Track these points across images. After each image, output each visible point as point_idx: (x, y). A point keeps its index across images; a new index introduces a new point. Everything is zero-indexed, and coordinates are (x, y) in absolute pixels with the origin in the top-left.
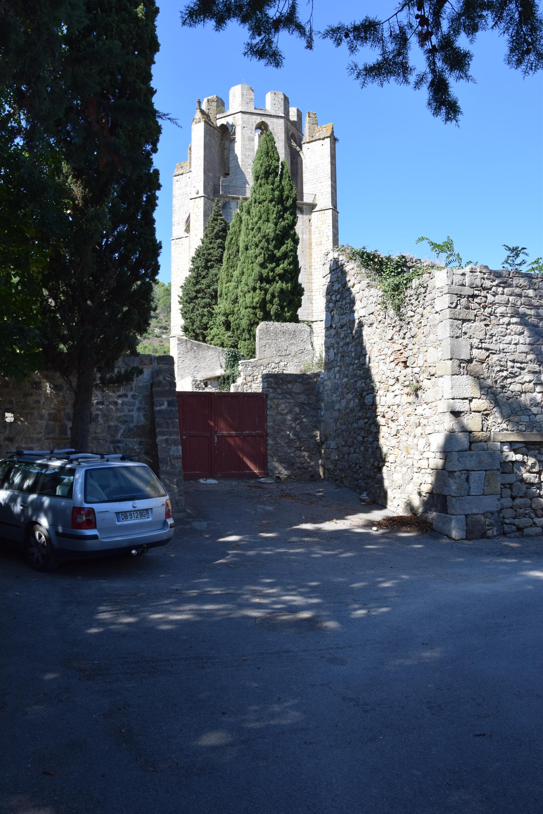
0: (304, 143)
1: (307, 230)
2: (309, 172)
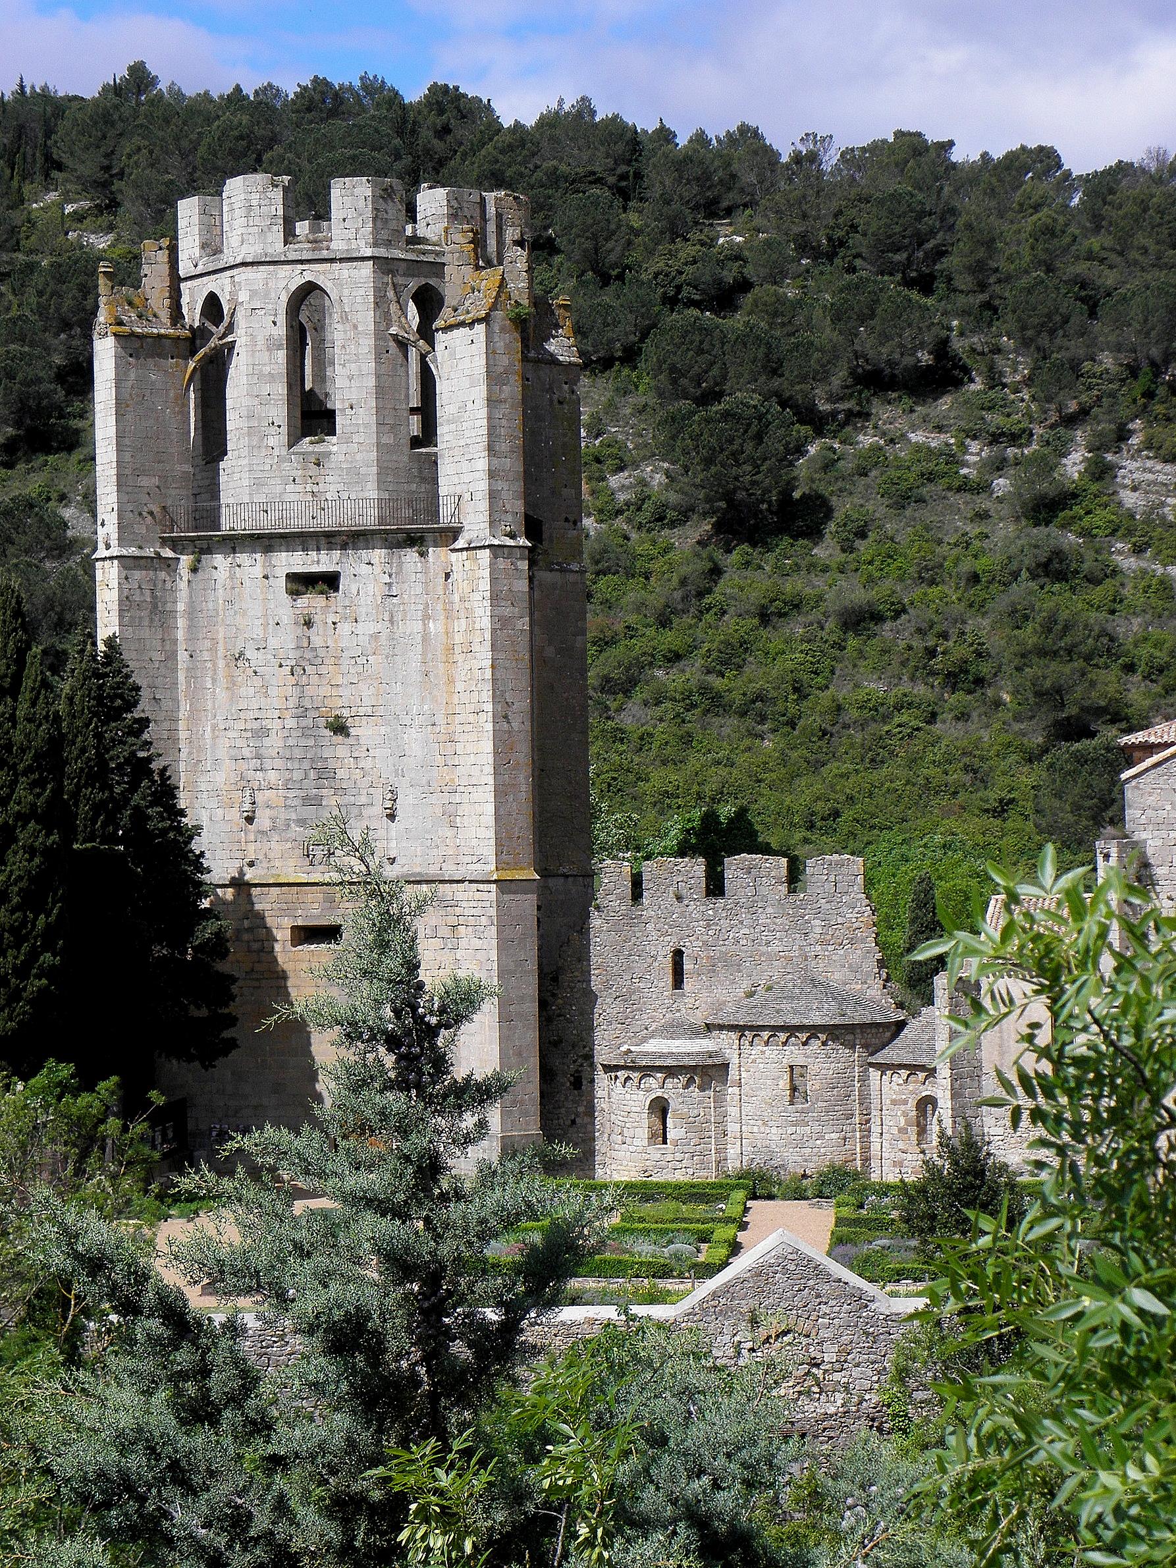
0: (437, 330)
1: (440, 607)
2: (449, 422)
